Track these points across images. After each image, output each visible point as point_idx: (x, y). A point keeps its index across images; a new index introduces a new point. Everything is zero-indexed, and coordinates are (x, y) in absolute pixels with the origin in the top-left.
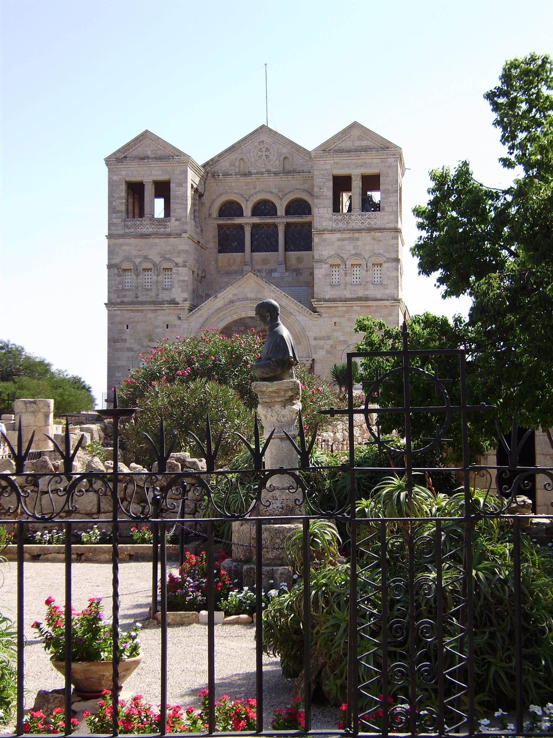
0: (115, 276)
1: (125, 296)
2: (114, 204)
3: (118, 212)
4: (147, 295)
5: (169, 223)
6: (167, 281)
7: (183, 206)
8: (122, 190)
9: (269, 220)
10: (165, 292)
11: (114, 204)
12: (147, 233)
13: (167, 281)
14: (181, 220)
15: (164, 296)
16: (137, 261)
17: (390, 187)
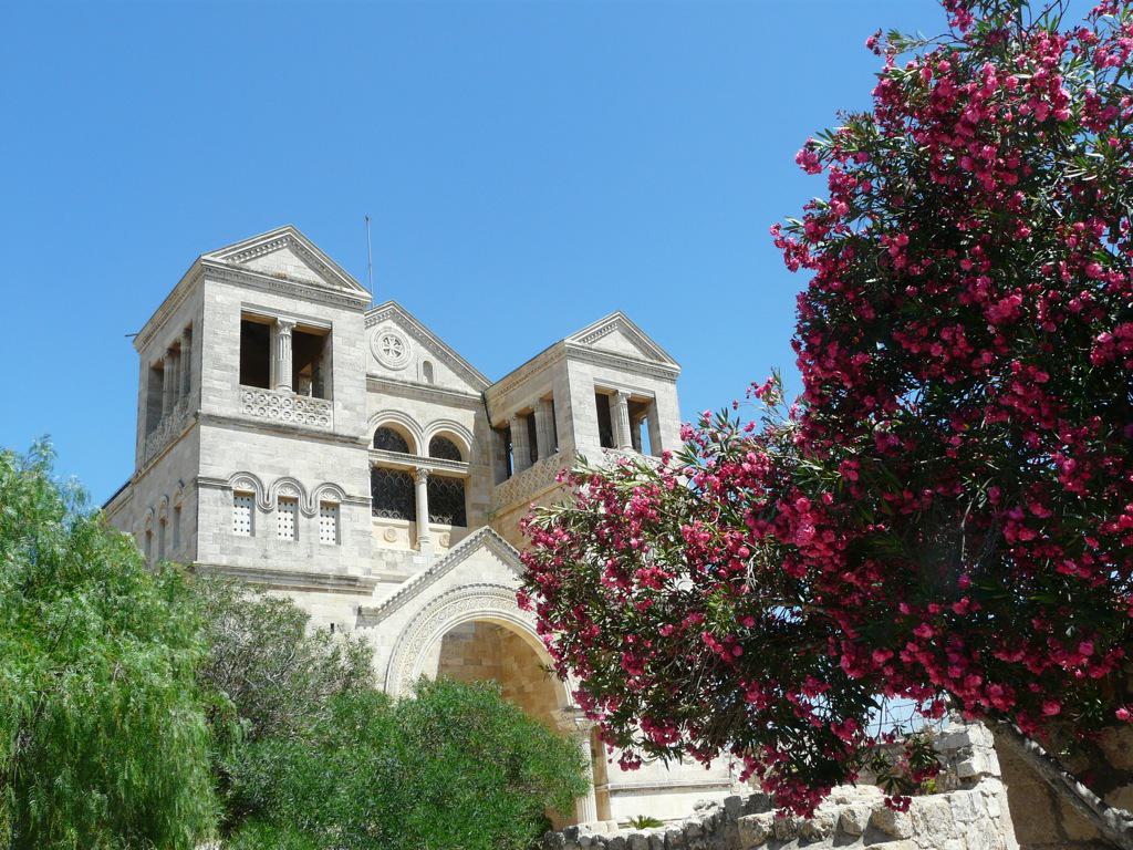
0: (216, 501)
1: (238, 551)
2: (218, 349)
3: (225, 367)
4: (288, 554)
5: (330, 411)
6: (325, 530)
7: (357, 384)
8: (234, 326)
9: (403, 463)
10: (324, 551)
11: (218, 349)
12: (287, 422)
13: (325, 530)
14: (355, 410)
15: (324, 564)
16: (267, 478)
17: (671, 423)
